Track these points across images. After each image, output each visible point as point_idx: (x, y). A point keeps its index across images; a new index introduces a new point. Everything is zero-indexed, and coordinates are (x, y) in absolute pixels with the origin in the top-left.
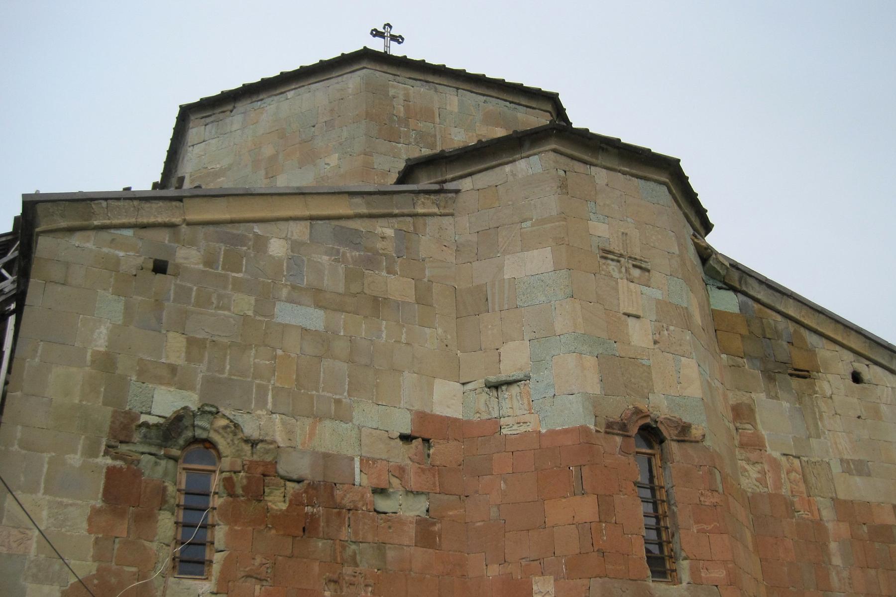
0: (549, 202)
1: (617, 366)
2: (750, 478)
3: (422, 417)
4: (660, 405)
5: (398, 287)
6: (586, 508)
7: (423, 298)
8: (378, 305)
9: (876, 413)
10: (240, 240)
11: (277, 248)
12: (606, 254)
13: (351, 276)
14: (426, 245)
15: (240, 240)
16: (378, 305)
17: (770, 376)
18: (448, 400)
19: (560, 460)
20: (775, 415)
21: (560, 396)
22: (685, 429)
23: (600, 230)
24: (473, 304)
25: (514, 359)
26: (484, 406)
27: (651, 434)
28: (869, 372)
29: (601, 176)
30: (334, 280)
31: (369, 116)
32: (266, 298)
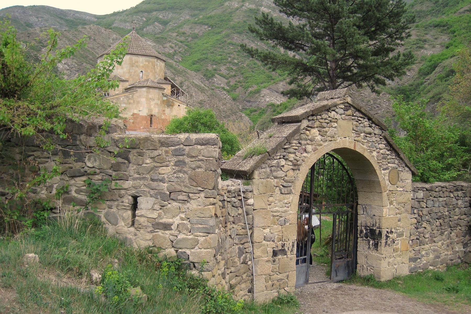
0: (145, 94)
1: (150, 110)
2: (163, 117)
3: (133, 113)
4: (153, 113)
5: (132, 101)
6: (145, 122)
7: (134, 102)
8: (130, 103)
9: (180, 109)
10: (118, 99)
11: (122, 99)
12: (150, 99)
13: (128, 101)
14: (135, 97)
15: (118, 99)
16: (130, 103)
17: (168, 107)
18: (136, 111)
19: (144, 118)
20: (167, 111)
21: (144, 112)
22: (155, 116)
23: (150, 96)
24: (138, 102)
25: (141, 108)
26: (138, 112)
27: (152, 116)
28: (180, 105)
29: (151, 90)
30: (126, 102)
31: (130, 64)
32: (121, 104)
